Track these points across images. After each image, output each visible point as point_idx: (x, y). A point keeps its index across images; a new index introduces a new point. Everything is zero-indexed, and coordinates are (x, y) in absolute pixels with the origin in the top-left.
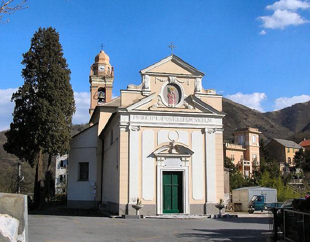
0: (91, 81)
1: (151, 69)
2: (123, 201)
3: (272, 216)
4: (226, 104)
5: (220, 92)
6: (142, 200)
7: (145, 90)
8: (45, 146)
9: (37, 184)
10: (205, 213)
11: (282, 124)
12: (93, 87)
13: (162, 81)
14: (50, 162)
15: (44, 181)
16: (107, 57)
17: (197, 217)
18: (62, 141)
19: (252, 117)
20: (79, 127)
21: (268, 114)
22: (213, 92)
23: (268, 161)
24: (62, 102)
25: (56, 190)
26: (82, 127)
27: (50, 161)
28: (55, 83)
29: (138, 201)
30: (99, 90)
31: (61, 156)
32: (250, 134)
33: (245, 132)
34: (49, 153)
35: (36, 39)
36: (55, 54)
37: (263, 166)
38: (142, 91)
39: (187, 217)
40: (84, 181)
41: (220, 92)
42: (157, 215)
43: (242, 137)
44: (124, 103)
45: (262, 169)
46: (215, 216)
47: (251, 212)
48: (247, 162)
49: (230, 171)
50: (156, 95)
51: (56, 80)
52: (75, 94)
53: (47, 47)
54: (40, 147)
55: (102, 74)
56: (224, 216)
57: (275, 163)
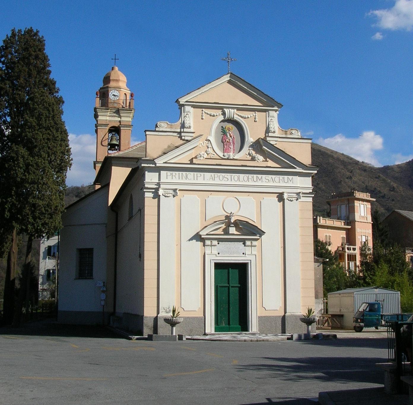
0: (96, 116)
1: (195, 96)
2: (149, 312)
3: (393, 335)
4: (319, 154)
5: (308, 134)
6: (180, 310)
7: (185, 130)
8: (21, 222)
9: (9, 283)
10: (284, 332)
11: (410, 186)
12: (102, 125)
13: (214, 116)
14: (31, 248)
15: (20, 279)
16: (123, 78)
17: (270, 337)
18: (50, 214)
19: (361, 175)
20: (77, 191)
21: (386, 170)
22: (297, 134)
23: (386, 246)
24: (50, 151)
25: (40, 293)
26: (83, 192)
27: (29, 247)
28: (39, 118)
29: (174, 311)
30: (110, 131)
31: (48, 238)
32: (357, 203)
33: (349, 200)
34: (28, 234)
35: (7, 48)
36: (39, 72)
37: (378, 254)
38: (180, 133)
39: (254, 338)
40: (86, 279)
41: (308, 134)
42: (205, 334)
43: (343, 207)
44: (152, 152)
45: (377, 258)
46: (300, 336)
47: (359, 329)
48: (352, 247)
49: (324, 263)
50: (204, 138)
51: (40, 114)
52: (71, 137)
53: (25, 60)
54: (14, 223)
55: (116, 105)
56: (315, 336)
57: (397, 250)
